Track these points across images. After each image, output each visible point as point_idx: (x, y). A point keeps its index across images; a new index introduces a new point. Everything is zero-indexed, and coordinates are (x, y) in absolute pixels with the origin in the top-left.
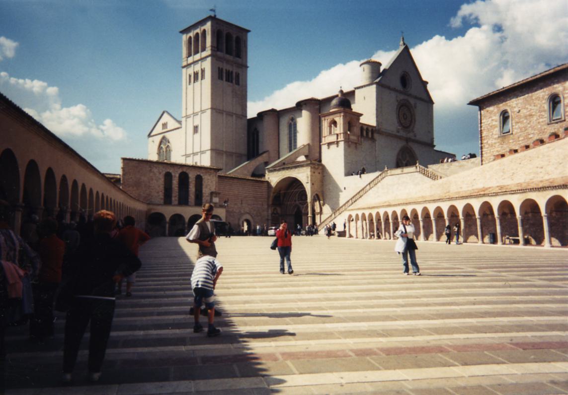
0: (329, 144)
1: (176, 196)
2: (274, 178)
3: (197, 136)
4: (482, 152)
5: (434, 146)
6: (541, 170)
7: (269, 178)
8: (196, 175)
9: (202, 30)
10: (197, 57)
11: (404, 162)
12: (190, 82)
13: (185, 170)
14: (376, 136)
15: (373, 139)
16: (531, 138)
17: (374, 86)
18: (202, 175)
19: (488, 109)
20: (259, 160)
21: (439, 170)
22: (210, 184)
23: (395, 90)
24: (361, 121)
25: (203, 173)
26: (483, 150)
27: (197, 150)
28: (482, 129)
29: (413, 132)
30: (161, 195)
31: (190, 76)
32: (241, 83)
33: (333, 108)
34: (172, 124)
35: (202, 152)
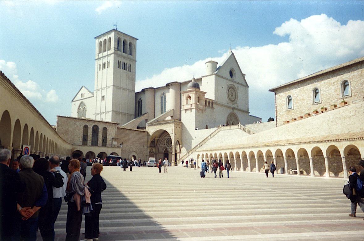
1: (90, 140)
2: (151, 130)
3: (104, 102)
4: (276, 119)
5: (249, 113)
6: (309, 131)
7: (148, 130)
8: (103, 127)
9: (108, 37)
10: (105, 54)
11: (231, 122)
12: (100, 69)
13: (96, 124)
14: (214, 105)
16: (303, 112)
17: (214, 76)
18: (107, 127)
19: (280, 94)
20: (141, 119)
21: (252, 128)
22: (112, 133)
23: (226, 79)
24: (205, 97)
25: (108, 126)
26: (277, 118)
27: (103, 111)
28: (277, 105)
29: (237, 104)
30: (81, 139)
31: (100, 65)
32: (131, 71)
33: (189, 89)
34: (87, 95)
35: (106, 112)
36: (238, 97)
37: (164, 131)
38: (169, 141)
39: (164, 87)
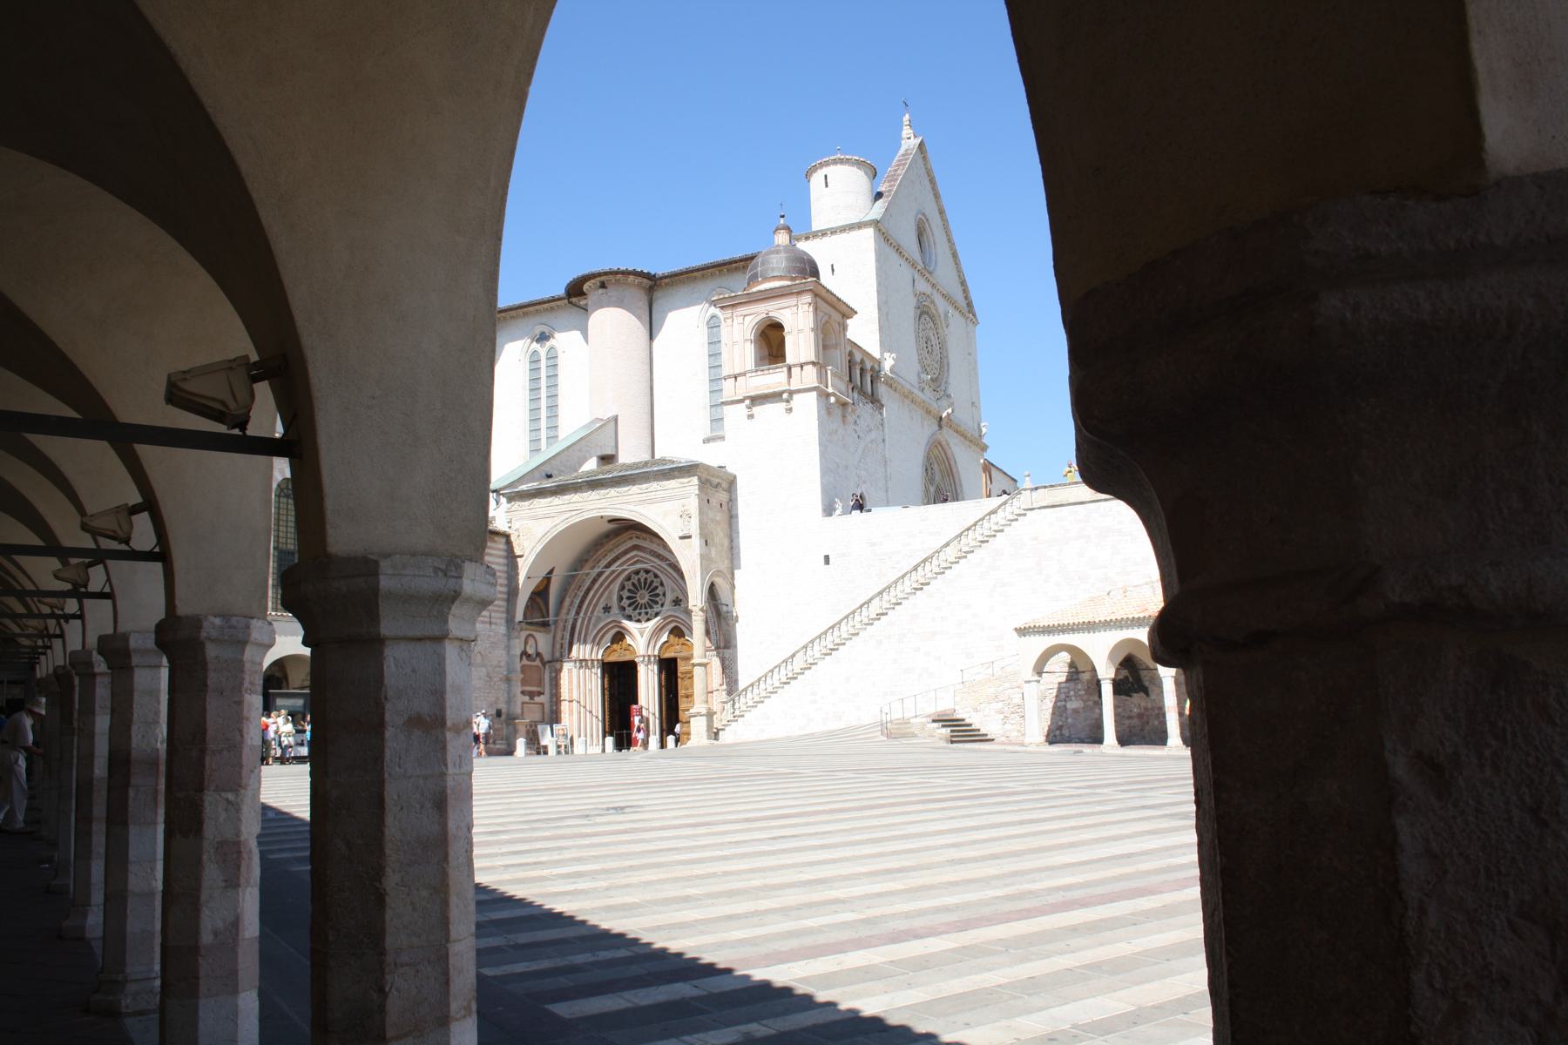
0: (757, 400)
5: (984, 448)
14: (882, 390)
15: (874, 399)
33: (766, 279)
36: (948, 364)
38: (636, 588)
39: (554, 300)
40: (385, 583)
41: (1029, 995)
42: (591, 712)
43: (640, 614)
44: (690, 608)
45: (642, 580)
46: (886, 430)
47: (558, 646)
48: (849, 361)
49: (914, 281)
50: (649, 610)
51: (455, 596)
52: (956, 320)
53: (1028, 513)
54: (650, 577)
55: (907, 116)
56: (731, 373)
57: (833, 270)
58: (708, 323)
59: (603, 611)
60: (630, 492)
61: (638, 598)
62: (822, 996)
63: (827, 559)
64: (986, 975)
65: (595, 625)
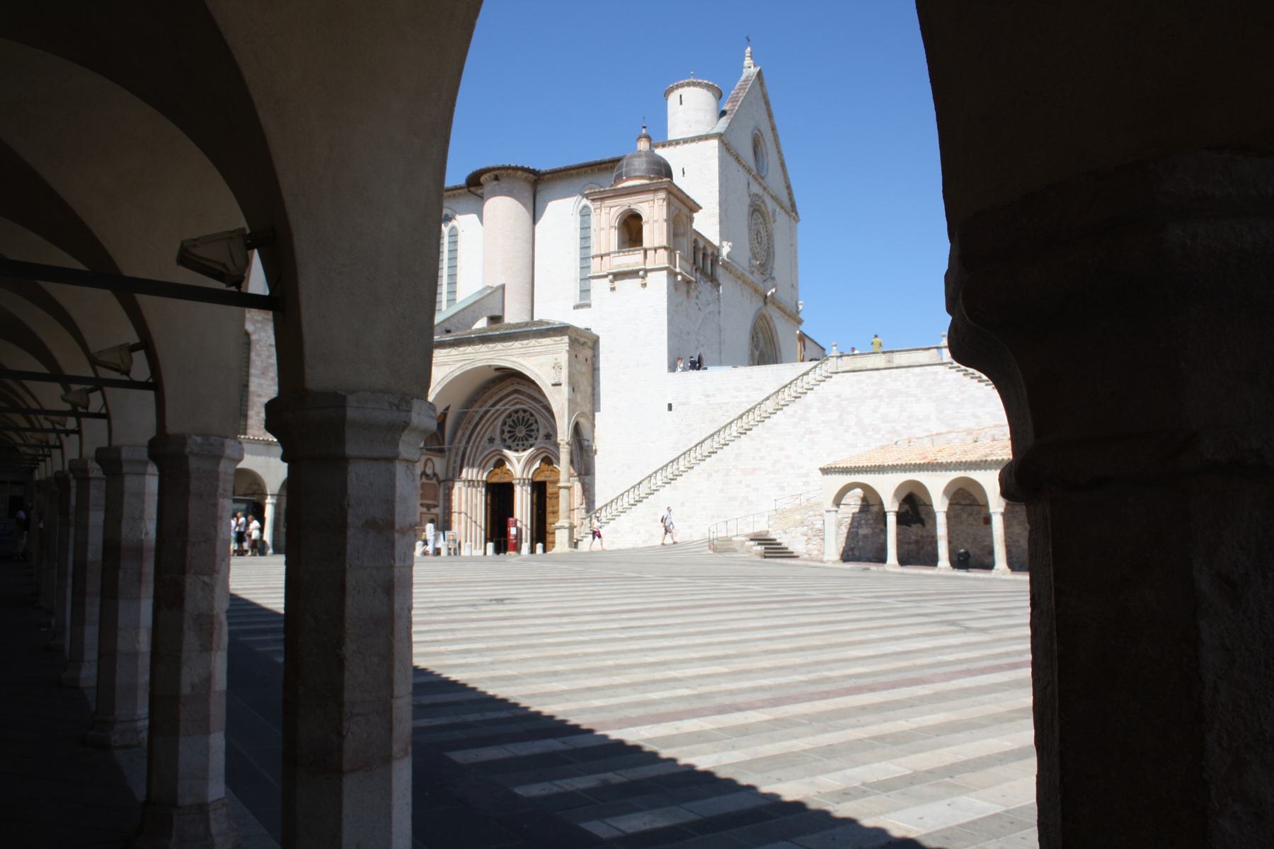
0: (618, 276)
5: (800, 322)
14: (720, 272)
15: (713, 280)
33: (629, 178)
36: (774, 253)
37: (497, 373)
38: (515, 425)
40: (351, 413)
41: (828, 758)
42: (476, 522)
43: (518, 445)
44: (559, 441)
45: (521, 418)
46: (722, 305)
47: (451, 469)
48: (694, 247)
49: (749, 184)
50: (525, 442)
51: (405, 426)
52: (781, 218)
53: (834, 376)
54: (527, 416)
55: (749, 49)
56: (598, 253)
57: (684, 173)
58: (581, 212)
59: (487, 441)
60: (513, 347)
61: (517, 433)
62: (665, 753)
63: (670, 407)
64: (794, 742)
65: (481, 453)
